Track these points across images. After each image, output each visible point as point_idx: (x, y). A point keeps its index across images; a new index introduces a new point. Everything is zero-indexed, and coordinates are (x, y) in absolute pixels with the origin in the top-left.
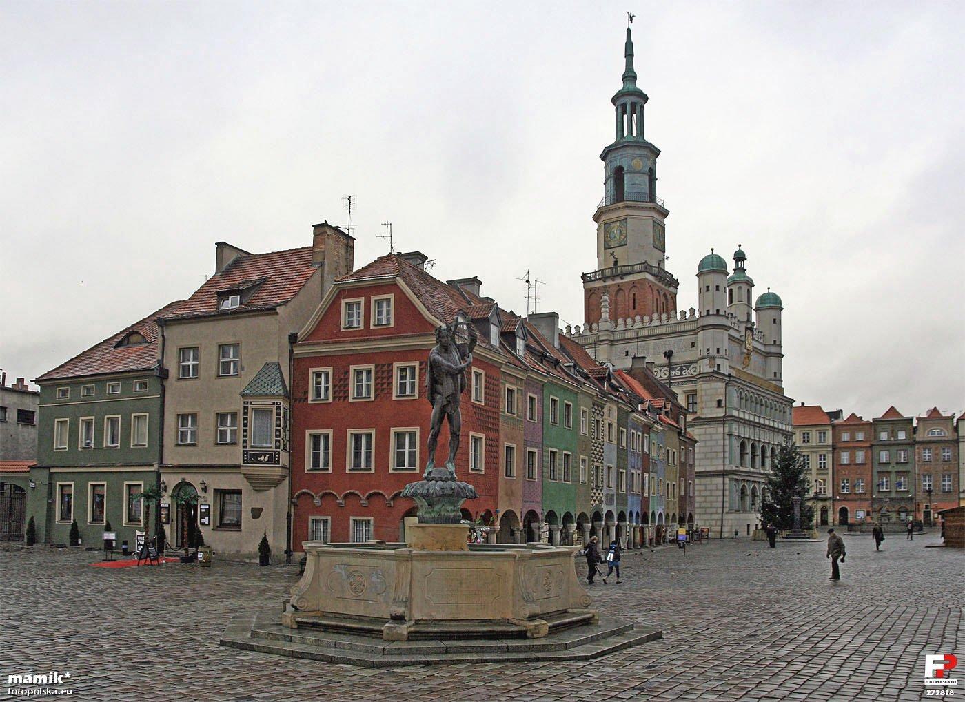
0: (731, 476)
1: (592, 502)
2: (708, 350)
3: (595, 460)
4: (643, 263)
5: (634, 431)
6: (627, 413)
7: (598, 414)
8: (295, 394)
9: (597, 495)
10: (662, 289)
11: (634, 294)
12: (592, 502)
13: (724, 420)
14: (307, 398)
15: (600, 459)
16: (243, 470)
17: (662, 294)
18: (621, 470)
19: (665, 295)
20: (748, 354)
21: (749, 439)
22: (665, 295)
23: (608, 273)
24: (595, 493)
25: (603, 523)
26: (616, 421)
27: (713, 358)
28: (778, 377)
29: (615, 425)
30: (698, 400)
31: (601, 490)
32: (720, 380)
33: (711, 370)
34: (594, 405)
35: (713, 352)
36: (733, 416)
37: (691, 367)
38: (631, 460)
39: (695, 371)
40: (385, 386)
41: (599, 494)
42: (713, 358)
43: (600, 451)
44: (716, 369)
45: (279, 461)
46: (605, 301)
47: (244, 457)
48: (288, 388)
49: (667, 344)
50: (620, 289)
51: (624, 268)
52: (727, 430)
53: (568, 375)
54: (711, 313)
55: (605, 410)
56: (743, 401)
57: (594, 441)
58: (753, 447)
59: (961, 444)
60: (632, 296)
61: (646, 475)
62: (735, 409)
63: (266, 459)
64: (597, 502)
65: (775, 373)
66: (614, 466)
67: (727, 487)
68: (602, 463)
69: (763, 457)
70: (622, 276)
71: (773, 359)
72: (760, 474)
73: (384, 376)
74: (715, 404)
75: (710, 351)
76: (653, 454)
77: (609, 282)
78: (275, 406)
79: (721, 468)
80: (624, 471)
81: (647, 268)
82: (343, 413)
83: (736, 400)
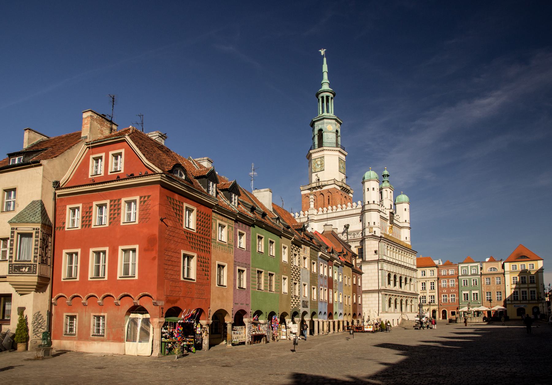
0: (383, 293)
7: (296, 251)
13: (378, 261)
14: (64, 227)
15: (297, 278)
16: (8, 279)
18: (313, 287)
31: (299, 298)
33: (371, 234)
38: (320, 281)
40: (116, 215)
44: (373, 233)
45: (36, 272)
47: (9, 269)
49: (345, 221)
59: (506, 275)
63: (27, 270)
67: (380, 299)
76: (336, 278)
82: (87, 237)
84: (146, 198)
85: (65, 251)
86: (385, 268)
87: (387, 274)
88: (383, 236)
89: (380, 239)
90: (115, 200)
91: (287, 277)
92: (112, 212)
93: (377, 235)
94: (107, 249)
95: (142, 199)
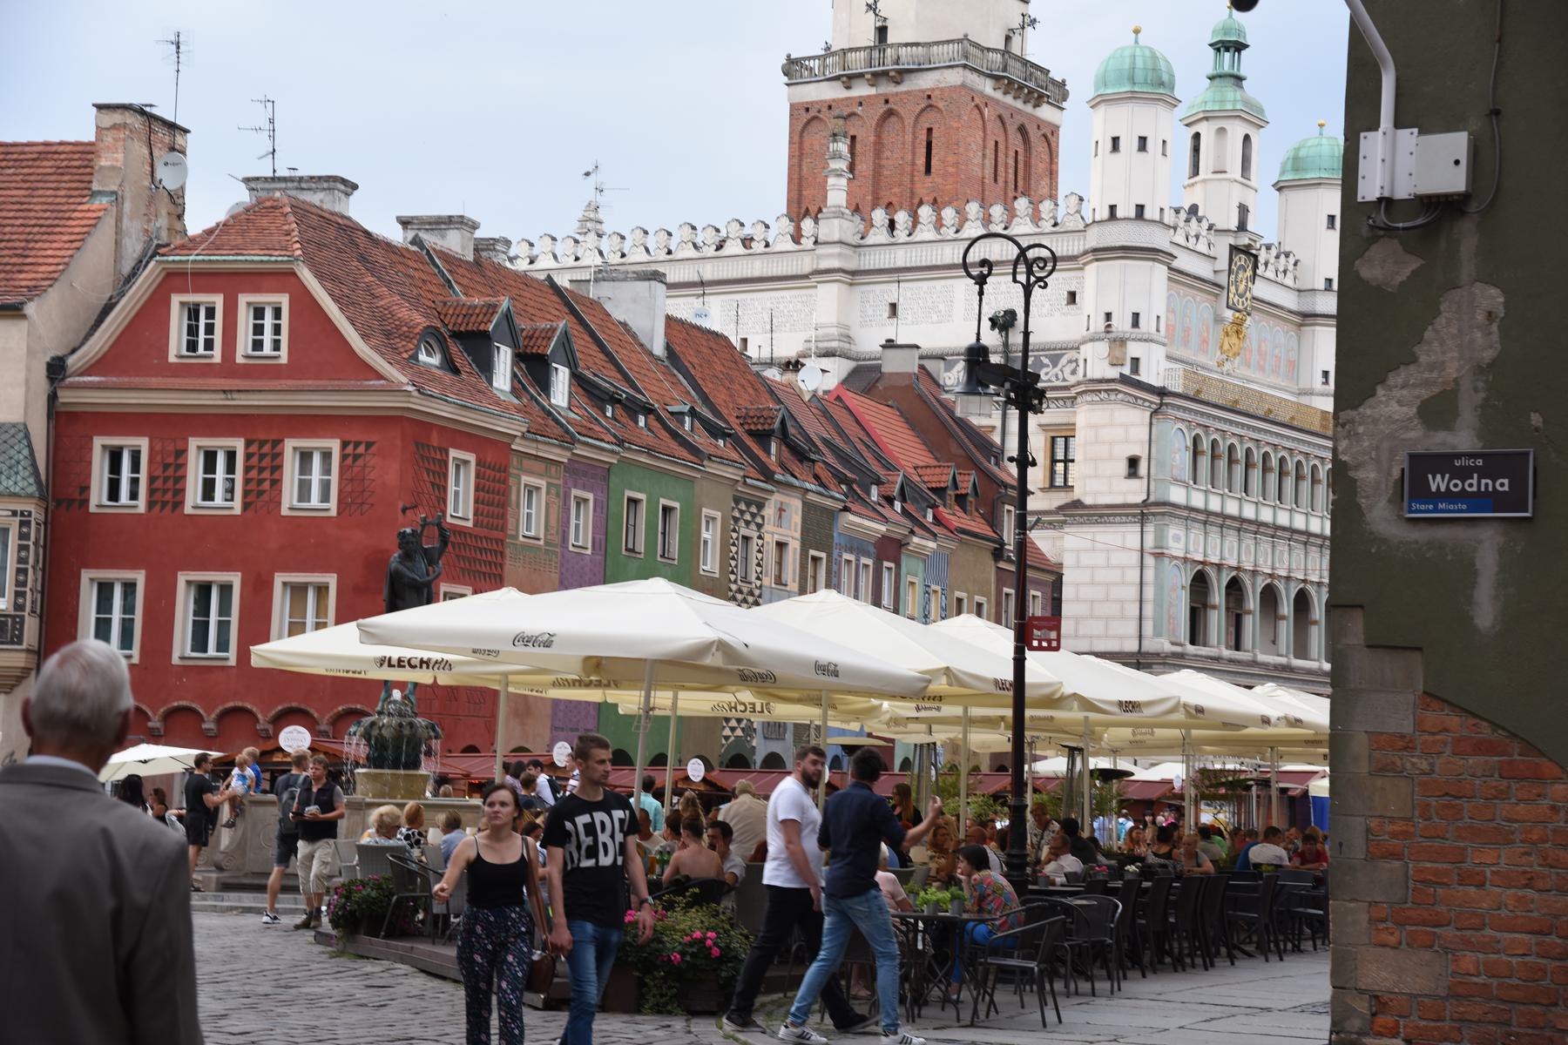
1: (727, 732)
2: (1108, 316)
4: (959, 41)
5: (851, 557)
6: (831, 515)
7: (747, 523)
8: (61, 490)
10: (1014, 113)
11: (930, 130)
12: (727, 732)
13: (1144, 513)
14: (87, 501)
17: (1012, 129)
19: (1022, 129)
20: (1238, 325)
21: (1219, 567)
22: (1022, 129)
23: (857, 62)
26: (798, 535)
27: (1122, 342)
29: (794, 546)
30: (1076, 452)
32: (1135, 402)
33: (1113, 373)
34: (737, 500)
35: (1122, 324)
37: (1063, 361)
39: (1074, 372)
40: (266, 485)
42: (1122, 342)
44: (1127, 371)
46: (837, 156)
48: (43, 478)
50: (890, 113)
51: (903, 51)
53: (675, 435)
54: (1120, 213)
55: (769, 511)
56: (1204, 462)
57: (734, 587)
58: (1235, 587)
60: (923, 137)
62: (1177, 481)
64: (739, 733)
70: (901, 75)
72: (1254, 663)
73: (264, 464)
74: (1123, 467)
75: (1114, 322)
77: (862, 90)
78: (18, 519)
79: (1132, 646)
81: (968, 52)
83: (1181, 459)
84: (361, 450)
85: (86, 575)
86: (1176, 549)
87: (1185, 578)
88: (1176, 386)
90: (262, 443)
92: (253, 474)
93: (1144, 376)
94: (235, 579)
95: (350, 449)
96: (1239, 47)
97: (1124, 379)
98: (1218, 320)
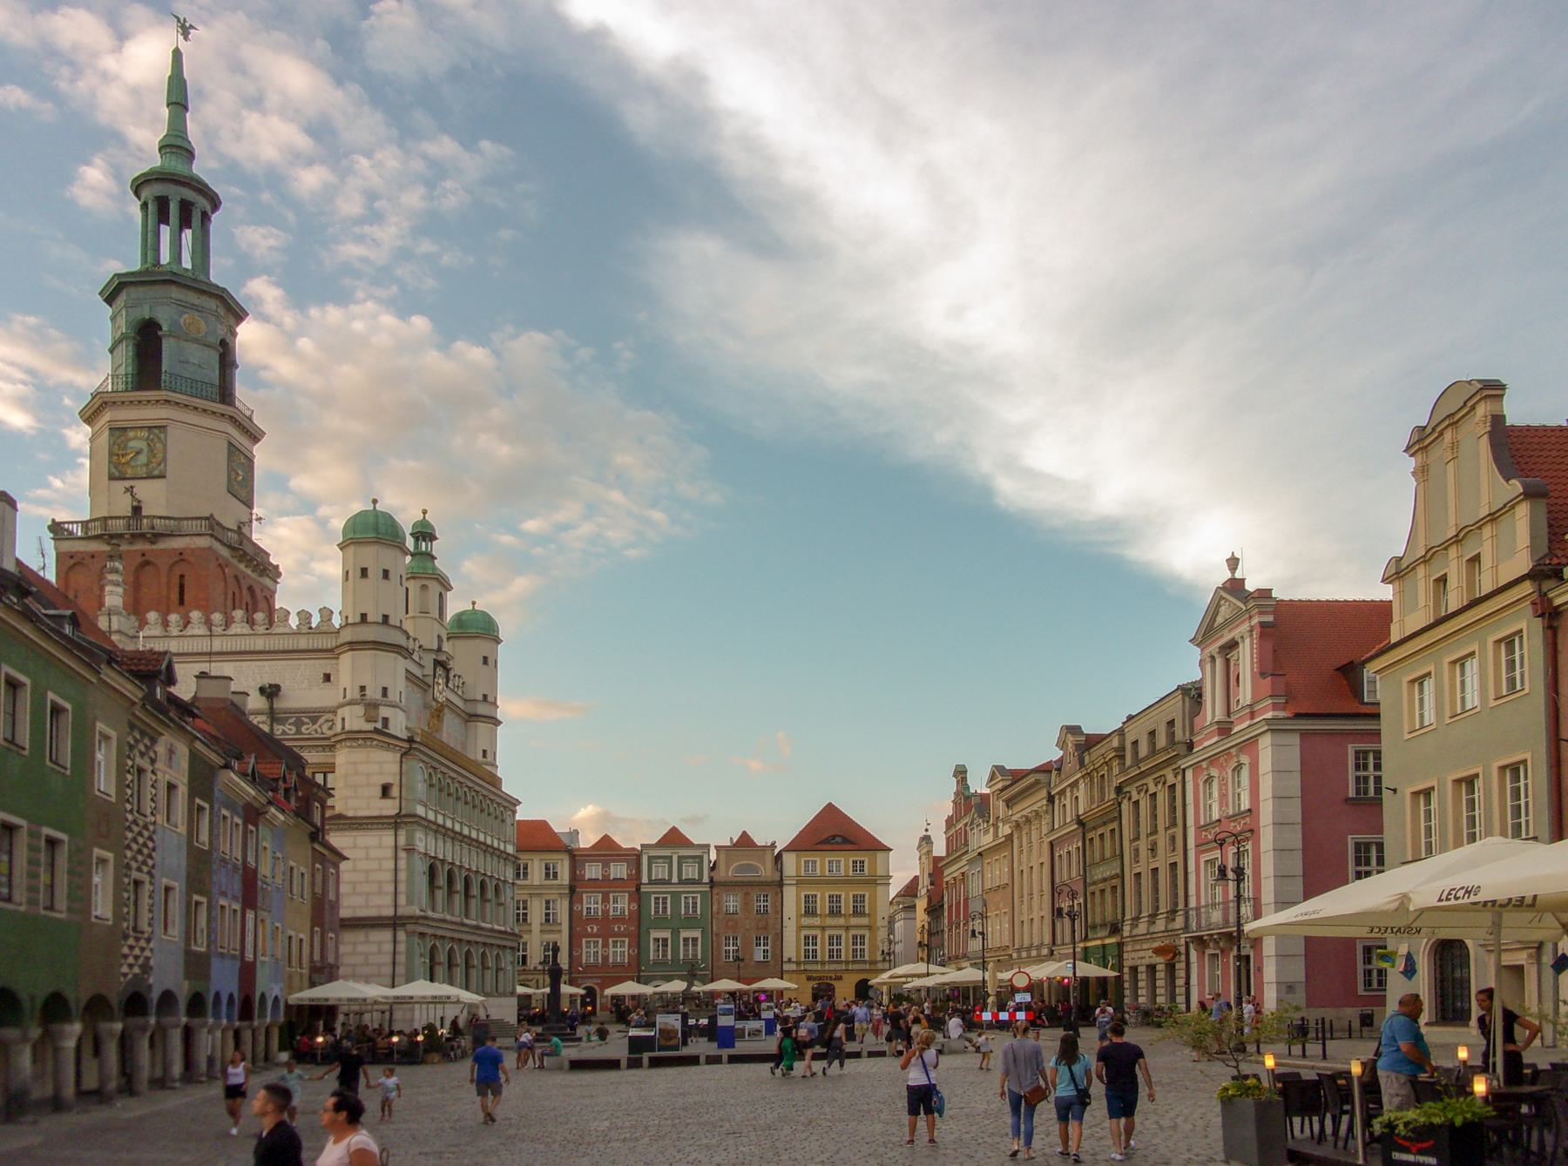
2: (363, 688)
3: (134, 865)
7: (142, 755)
9: (137, 951)
12: (125, 969)
13: (396, 822)
18: (196, 897)
24: (131, 948)
25: (153, 1020)
28: (489, 758)
29: (183, 790)
31: (148, 940)
32: (388, 747)
33: (369, 727)
34: (132, 727)
35: (373, 693)
36: (415, 816)
41: (143, 949)
43: (145, 845)
44: (379, 725)
52: (402, 840)
55: (161, 748)
57: (130, 817)
61: (250, 915)
62: (420, 802)
64: (136, 970)
65: (485, 752)
66: (178, 886)
68: (149, 873)
69: (467, 895)
71: (482, 727)
74: (379, 792)
75: (368, 692)
80: (204, 900)
83: (421, 788)
89: (409, 747)
91: (109, 855)
96: (432, 537)
97: (376, 731)
98: (426, 706)
